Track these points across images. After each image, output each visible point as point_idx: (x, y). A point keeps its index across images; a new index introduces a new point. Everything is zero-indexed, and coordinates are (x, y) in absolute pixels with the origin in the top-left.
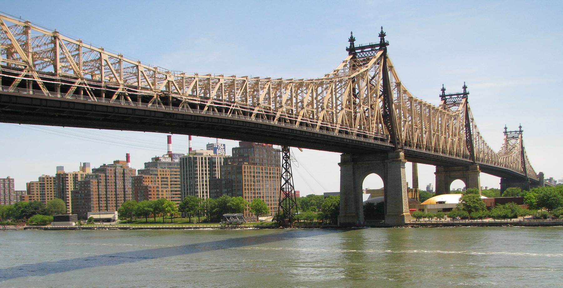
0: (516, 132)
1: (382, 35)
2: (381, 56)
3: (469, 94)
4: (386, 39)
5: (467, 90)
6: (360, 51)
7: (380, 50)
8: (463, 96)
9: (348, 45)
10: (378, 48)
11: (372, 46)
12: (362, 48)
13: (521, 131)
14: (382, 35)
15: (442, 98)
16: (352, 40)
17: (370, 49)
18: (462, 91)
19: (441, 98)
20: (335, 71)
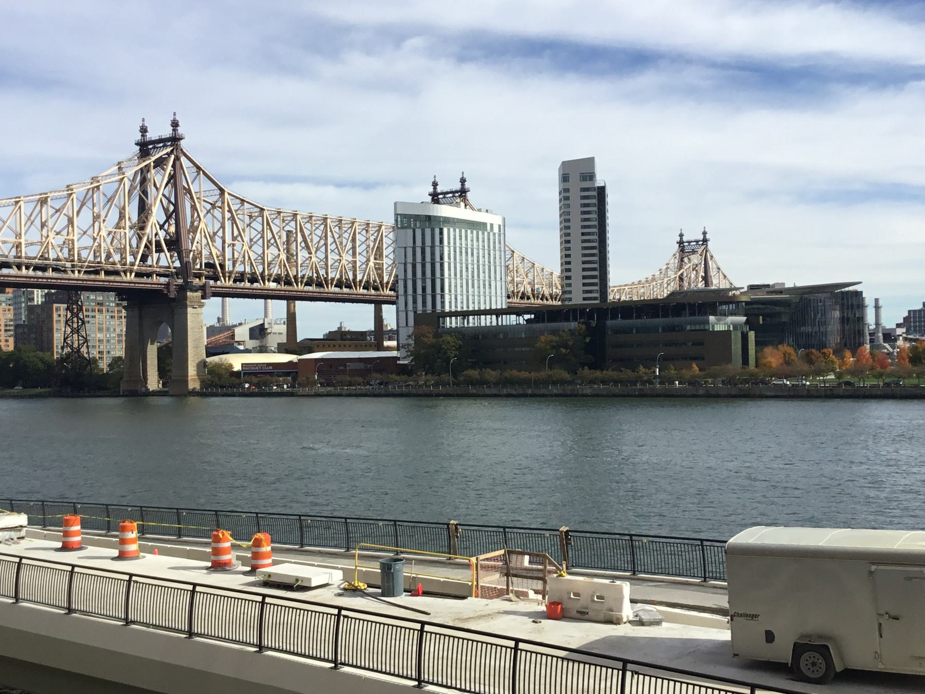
0: (697, 242)
1: (175, 124)
2: (169, 154)
3: (468, 191)
4: (180, 130)
5: (467, 185)
6: (150, 147)
7: (171, 146)
8: (461, 194)
9: (139, 137)
10: (169, 143)
13: (705, 241)
14: (175, 124)
15: (432, 198)
16: (144, 130)
17: (161, 145)
18: (458, 186)
19: (431, 197)
20: (92, 179)
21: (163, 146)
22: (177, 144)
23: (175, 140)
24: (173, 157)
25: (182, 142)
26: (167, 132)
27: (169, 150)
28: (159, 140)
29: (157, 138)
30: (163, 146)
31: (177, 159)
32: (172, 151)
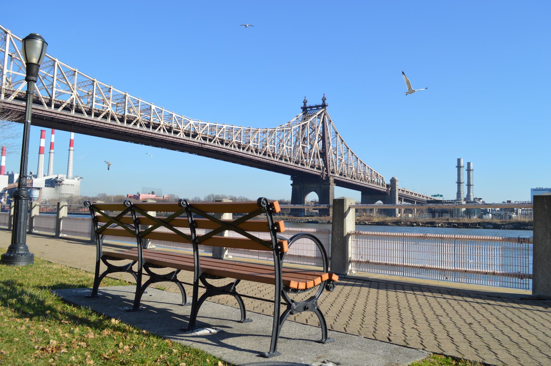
1: (324, 100)
2: (322, 113)
4: (326, 102)
6: (308, 109)
7: (321, 109)
10: (321, 108)
11: (317, 107)
12: (311, 107)
14: (324, 100)
17: (316, 108)
21: (317, 109)
22: (325, 108)
23: (324, 106)
24: (323, 114)
25: (326, 107)
26: (321, 103)
27: (322, 110)
28: (315, 106)
29: (315, 105)
30: (317, 109)
31: (325, 114)
32: (323, 111)
